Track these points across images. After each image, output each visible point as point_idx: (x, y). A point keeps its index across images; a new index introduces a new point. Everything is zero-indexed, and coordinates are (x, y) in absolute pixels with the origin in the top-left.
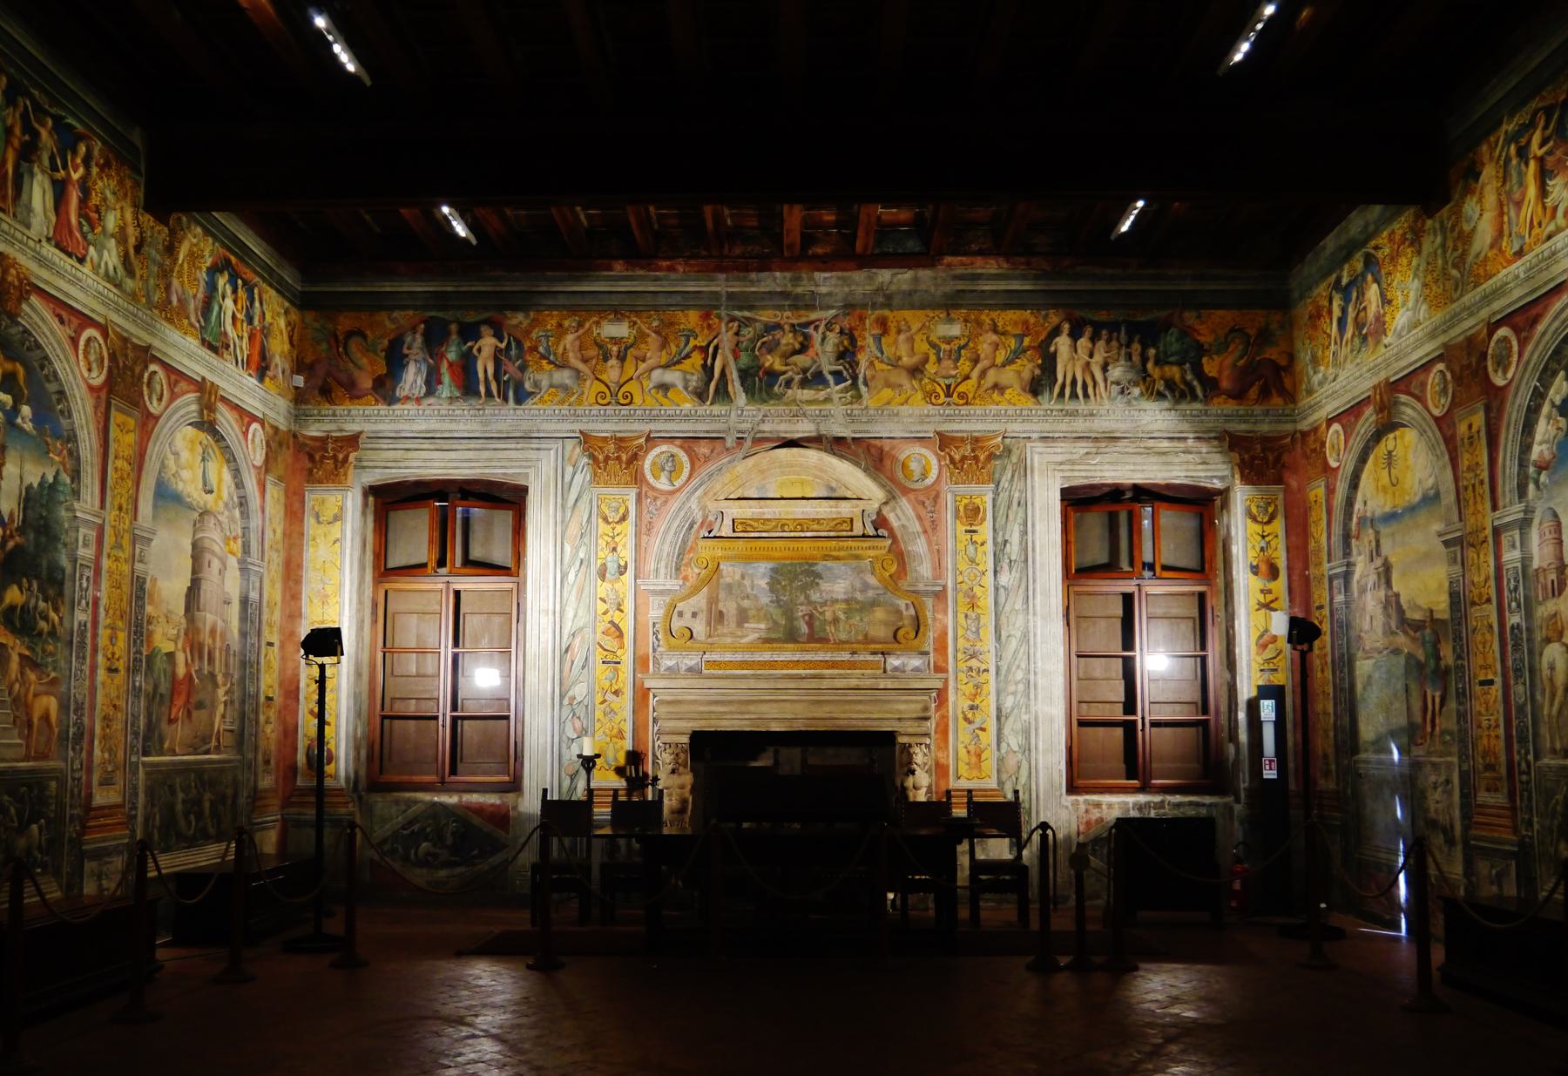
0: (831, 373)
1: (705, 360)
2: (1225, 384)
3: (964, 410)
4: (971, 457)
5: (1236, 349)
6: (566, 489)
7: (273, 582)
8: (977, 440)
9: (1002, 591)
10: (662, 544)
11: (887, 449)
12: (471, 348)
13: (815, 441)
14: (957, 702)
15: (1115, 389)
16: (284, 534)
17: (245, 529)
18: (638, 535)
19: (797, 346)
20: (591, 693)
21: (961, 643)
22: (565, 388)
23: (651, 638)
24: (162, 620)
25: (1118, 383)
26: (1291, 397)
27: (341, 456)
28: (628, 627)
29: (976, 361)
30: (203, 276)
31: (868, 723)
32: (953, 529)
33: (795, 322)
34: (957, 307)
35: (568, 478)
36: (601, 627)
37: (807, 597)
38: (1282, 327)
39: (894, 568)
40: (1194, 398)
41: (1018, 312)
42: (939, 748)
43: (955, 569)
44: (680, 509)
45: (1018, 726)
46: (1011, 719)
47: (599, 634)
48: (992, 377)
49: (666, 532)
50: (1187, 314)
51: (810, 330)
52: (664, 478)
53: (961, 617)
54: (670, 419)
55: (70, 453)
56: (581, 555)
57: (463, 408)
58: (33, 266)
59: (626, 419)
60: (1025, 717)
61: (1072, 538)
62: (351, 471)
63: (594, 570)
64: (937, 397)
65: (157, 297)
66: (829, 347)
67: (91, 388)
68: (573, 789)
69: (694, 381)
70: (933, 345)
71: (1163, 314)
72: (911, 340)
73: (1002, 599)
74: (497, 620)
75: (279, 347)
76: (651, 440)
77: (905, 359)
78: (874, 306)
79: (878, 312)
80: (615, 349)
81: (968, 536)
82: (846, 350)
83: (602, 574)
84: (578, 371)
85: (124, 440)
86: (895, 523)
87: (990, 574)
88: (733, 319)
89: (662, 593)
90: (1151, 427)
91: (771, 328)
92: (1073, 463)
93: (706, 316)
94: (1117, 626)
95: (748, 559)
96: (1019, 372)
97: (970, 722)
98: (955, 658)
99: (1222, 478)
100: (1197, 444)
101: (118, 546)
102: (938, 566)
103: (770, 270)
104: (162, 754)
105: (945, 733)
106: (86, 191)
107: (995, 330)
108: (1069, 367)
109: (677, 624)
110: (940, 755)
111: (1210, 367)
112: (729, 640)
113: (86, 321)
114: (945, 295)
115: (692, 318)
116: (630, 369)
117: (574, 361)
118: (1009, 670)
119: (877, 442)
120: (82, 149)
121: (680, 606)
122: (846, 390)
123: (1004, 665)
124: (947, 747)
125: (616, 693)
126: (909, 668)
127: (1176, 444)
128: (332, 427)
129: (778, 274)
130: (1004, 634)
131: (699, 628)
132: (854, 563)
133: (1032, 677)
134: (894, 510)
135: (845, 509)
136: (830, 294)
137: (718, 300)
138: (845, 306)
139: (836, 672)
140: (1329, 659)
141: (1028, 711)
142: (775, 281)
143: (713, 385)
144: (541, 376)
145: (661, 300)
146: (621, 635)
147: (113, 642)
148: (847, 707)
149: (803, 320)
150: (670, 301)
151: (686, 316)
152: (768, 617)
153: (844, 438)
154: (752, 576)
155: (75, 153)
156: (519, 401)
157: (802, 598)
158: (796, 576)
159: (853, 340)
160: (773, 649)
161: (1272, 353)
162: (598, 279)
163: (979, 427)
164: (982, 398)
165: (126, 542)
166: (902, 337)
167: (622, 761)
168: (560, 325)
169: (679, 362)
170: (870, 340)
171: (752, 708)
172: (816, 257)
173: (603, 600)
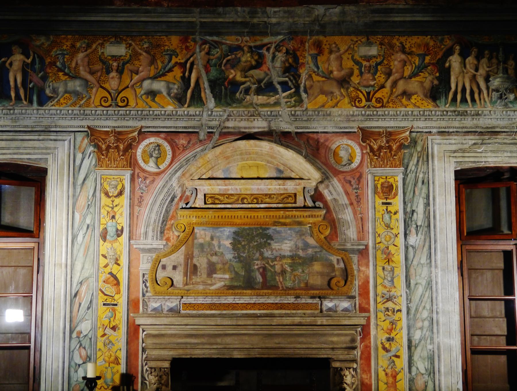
0: (280, 83)
4: (386, 147)
6: (76, 170)
8: (390, 134)
9: (410, 249)
10: (150, 213)
11: (322, 141)
12: (5, 62)
14: (377, 335)
15: (495, 95)
19: (254, 63)
20: (94, 329)
21: (380, 290)
22: (76, 93)
23: (141, 286)
25: (497, 90)
28: (123, 277)
29: (389, 74)
31: (308, 352)
32: (372, 202)
33: (252, 44)
34: (374, 33)
35: (78, 162)
37: (262, 254)
39: (328, 232)
41: (421, 38)
42: (364, 371)
43: (375, 233)
44: (164, 186)
45: (425, 354)
46: (419, 349)
47: (101, 283)
48: (401, 86)
51: (264, 51)
52: (152, 163)
53: (379, 269)
54: (156, 117)
56: (88, 221)
59: (124, 117)
60: (430, 347)
61: (464, 208)
63: (97, 233)
64: (360, 101)
66: (278, 64)
70: (357, 63)
72: (340, 58)
74: (22, 271)
76: (142, 134)
78: (312, 33)
80: (115, 64)
81: (384, 207)
82: (291, 66)
83: (104, 236)
84: (87, 81)
86: (329, 198)
87: (401, 236)
88: (205, 42)
89: (150, 251)
91: (233, 49)
92: (464, 151)
93: (184, 40)
95: (216, 225)
96: (422, 83)
97: (387, 350)
98: (376, 300)
102: (362, 231)
103: (233, 5)
105: (368, 359)
107: (403, 50)
108: (460, 78)
109: (161, 275)
110: (364, 376)
112: (201, 287)
115: (175, 41)
116: (126, 81)
117: (83, 73)
118: (417, 310)
119: (315, 136)
121: (164, 261)
122: (290, 96)
125: (114, 328)
126: (340, 309)
129: (239, 9)
130: (413, 282)
131: (178, 278)
132: (297, 228)
133: (435, 316)
134: (327, 187)
135: (290, 187)
136: (278, 24)
138: (290, 33)
139: (283, 312)
146: (118, 284)
148: (293, 339)
149: (258, 43)
151: (169, 40)
152: (231, 269)
153: (289, 133)
154: (219, 238)
156: (41, 103)
157: (257, 255)
158: (252, 238)
160: (235, 294)
163: (392, 124)
166: (333, 56)
168: (73, 46)
169: (164, 75)
170: (310, 59)
171: (219, 340)
173: (105, 256)
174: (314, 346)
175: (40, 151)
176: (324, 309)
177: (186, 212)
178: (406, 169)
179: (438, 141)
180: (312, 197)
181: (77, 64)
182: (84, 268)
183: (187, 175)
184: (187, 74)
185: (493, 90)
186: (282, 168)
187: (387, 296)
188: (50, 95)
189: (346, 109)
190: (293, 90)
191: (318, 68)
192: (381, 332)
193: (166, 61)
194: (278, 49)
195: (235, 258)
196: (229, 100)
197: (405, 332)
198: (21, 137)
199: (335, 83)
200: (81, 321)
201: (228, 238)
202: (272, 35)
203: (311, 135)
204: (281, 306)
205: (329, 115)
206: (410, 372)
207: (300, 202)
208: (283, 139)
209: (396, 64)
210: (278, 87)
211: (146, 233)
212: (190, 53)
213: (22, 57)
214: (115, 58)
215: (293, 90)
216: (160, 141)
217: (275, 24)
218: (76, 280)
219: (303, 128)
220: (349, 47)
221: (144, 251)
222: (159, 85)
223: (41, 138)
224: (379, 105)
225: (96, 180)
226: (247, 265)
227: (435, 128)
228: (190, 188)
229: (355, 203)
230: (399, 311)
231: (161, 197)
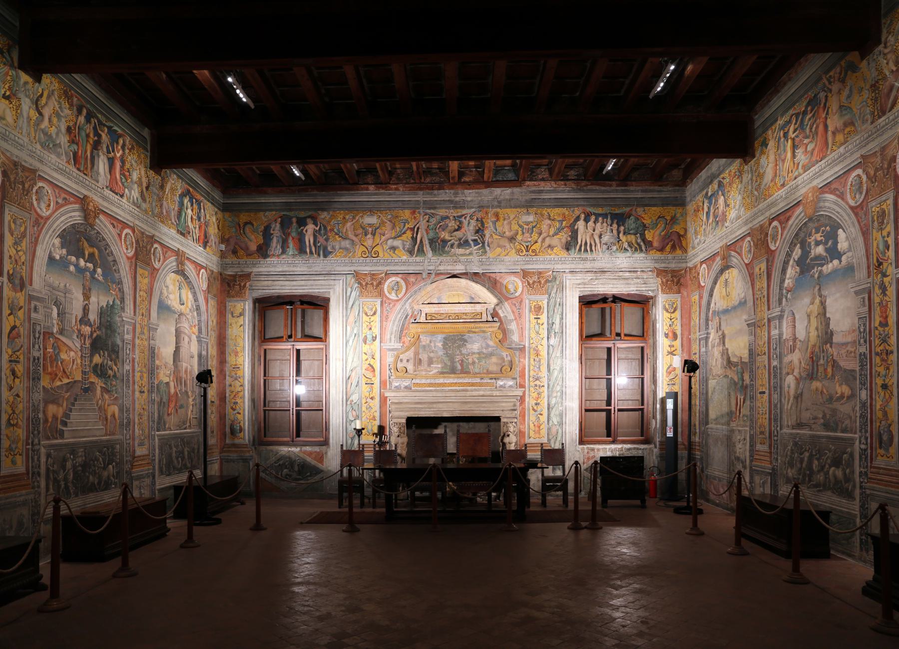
2: (655, 244)
3: (535, 258)
4: (539, 282)
5: (661, 226)
8: (540, 273)
10: (392, 326)
13: (464, 275)
14: (530, 401)
15: (605, 247)
17: (199, 321)
18: (381, 322)
20: (360, 399)
21: (532, 373)
22: (346, 249)
23: (388, 372)
24: (163, 367)
26: (685, 250)
28: (377, 367)
29: (540, 234)
30: (177, 199)
32: (528, 317)
34: (532, 207)
35: (348, 294)
36: (366, 366)
37: (461, 351)
39: (501, 337)
40: (641, 250)
43: (530, 337)
49: (394, 321)
50: (638, 209)
52: (393, 294)
53: (532, 360)
54: (396, 264)
55: (120, 290)
57: (299, 260)
58: (100, 201)
59: (376, 264)
61: (584, 321)
63: (361, 339)
65: (157, 211)
66: (471, 228)
67: (128, 258)
68: (352, 444)
69: (408, 245)
70: (520, 226)
71: (628, 209)
72: (510, 223)
73: (551, 352)
74: (316, 363)
75: (213, 231)
76: (388, 275)
78: (493, 207)
79: (495, 210)
83: (365, 341)
85: (143, 282)
87: (546, 339)
89: (392, 350)
90: (621, 266)
92: (585, 284)
94: (604, 362)
95: (433, 334)
97: (535, 411)
101: (143, 333)
102: (522, 335)
104: (165, 430)
105: (524, 416)
106: (123, 162)
109: (400, 365)
111: (649, 236)
113: (125, 225)
114: (526, 201)
116: (377, 241)
117: (351, 236)
119: (493, 275)
120: (121, 141)
121: (401, 356)
123: (551, 384)
125: (372, 398)
128: (238, 270)
130: (552, 368)
131: (410, 367)
132: (482, 334)
135: (478, 308)
136: (472, 201)
141: (562, 406)
144: (335, 243)
145: (392, 205)
146: (374, 371)
147: (140, 379)
150: (396, 205)
152: (442, 362)
155: (118, 143)
156: (325, 256)
158: (454, 341)
159: (483, 224)
160: (444, 377)
161: (677, 228)
162: (362, 195)
163: (542, 266)
165: (145, 331)
167: (376, 431)
169: (400, 236)
171: (435, 406)
172: (464, 182)
177: (415, 325)
182: (353, 361)
189: (513, 256)
194: (471, 217)
204: (473, 385)
207: (484, 319)
209: (544, 227)
214: (370, 225)
216: (398, 279)
221: (390, 350)
222: (397, 243)
226: (452, 359)
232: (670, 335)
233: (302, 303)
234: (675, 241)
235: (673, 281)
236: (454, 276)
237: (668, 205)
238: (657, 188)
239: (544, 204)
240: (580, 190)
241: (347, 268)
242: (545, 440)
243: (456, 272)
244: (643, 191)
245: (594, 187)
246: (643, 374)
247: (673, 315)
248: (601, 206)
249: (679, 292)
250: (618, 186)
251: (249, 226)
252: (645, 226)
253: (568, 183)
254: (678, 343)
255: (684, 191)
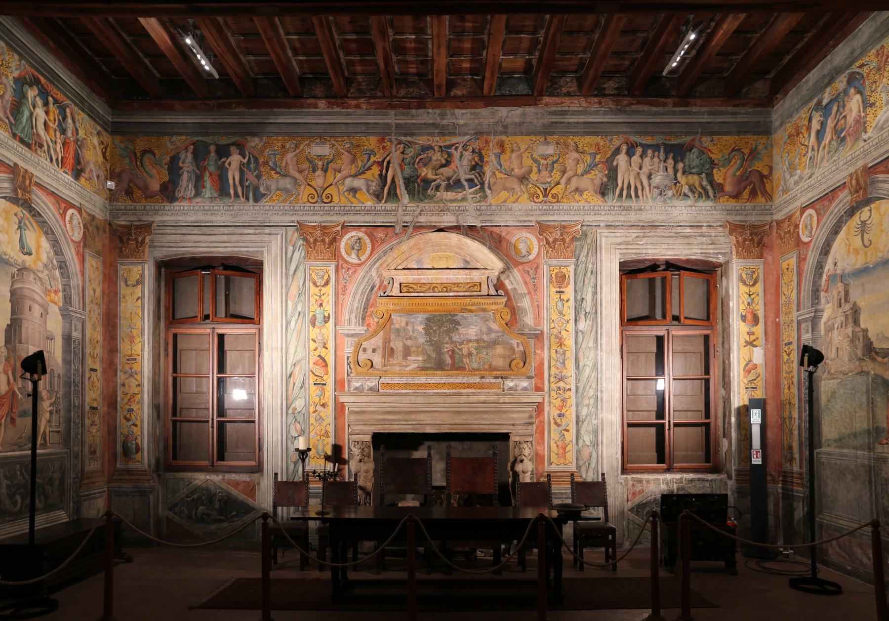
1: (381, 172)
2: (728, 188)
4: (562, 239)
5: (736, 163)
6: (289, 261)
7: (94, 328)
8: (564, 227)
9: (580, 334)
10: (352, 302)
11: (503, 234)
12: (224, 162)
13: (456, 229)
14: (551, 412)
15: (656, 191)
16: (103, 293)
19: (444, 162)
20: (307, 405)
21: (553, 371)
22: (287, 190)
23: (346, 367)
25: (658, 188)
26: (769, 197)
27: (140, 239)
31: (491, 427)
32: (548, 290)
33: (442, 144)
34: (552, 133)
35: (289, 255)
37: (450, 338)
38: (766, 148)
40: (708, 197)
41: (593, 138)
42: (538, 443)
43: (549, 319)
46: (586, 423)
47: (311, 365)
48: (574, 182)
49: (355, 294)
50: (704, 139)
51: (453, 150)
52: (354, 256)
53: (553, 352)
54: (357, 212)
56: (299, 309)
57: (219, 205)
59: (329, 213)
60: (595, 422)
62: (147, 249)
63: (307, 319)
64: (538, 197)
66: (465, 162)
68: (295, 472)
69: (374, 186)
70: (536, 161)
71: (688, 139)
72: (520, 157)
76: (345, 228)
77: (516, 170)
80: (320, 163)
82: (477, 164)
83: (313, 323)
84: (296, 179)
86: (509, 287)
87: (572, 322)
89: (353, 336)
93: (382, 140)
95: (410, 312)
97: (558, 425)
98: (549, 381)
99: (724, 254)
100: (709, 230)
102: (538, 316)
103: (425, 108)
105: (542, 433)
107: (577, 151)
108: (626, 176)
109: (362, 357)
111: (718, 177)
114: (544, 125)
117: (293, 172)
118: (584, 389)
121: (365, 344)
122: (476, 192)
124: (543, 443)
125: (323, 405)
126: (520, 388)
127: (695, 230)
128: (134, 218)
129: (430, 111)
131: (377, 360)
132: (482, 314)
133: (599, 394)
134: (508, 277)
135: (476, 276)
136: (465, 125)
137: (389, 129)
138: (476, 134)
139: (470, 391)
140: (795, 380)
141: (597, 418)
142: (426, 116)
143: (386, 188)
144: (270, 182)
145: (351, 129)
146: (326, 365)
148: (478, 416)
149: (448, 143)
150: (357, 130)
151: (368, 140)
152: (425, 352)
154: (413, 323)
156: (256, 200)
157: (447, 339)
158: (442, 323)
159: (481, 157)
160: (427, 375)
161: (758, 166)
162: (309, 114)
163: (566, 218)
164: (568, 198)
166: (514, 155)
167: (329, 453)
169: (363, 173)
170: (493, 157)
171: (413, 417)
172: (456, 97)
174: (497, 422)
175: (256, 244)
176: (506, 388)
177: (384, 300)
178: (578, 260)
179: (605, 234)
180: (495, 286)
181: (287, 163)
182: (296, 352)
183: (385, 265)
184: (384, 172)
185: (654, 187)
186: (468, 259)
187: (559, 377)
188: (264, 192)
189: (525, 203)
190: (478, 187)
191: (501, 166)
192: (553, 409)
193: (366, 160)
194: (465, 148)
195: (427, 341)
196: (421, 196)
197: (573, 408)
198: (239, 232)
199: (516, 180)
200: (295, 399)
201: (421, 323)
202: (460, 135)
203: (494, 229)
204: (468, 386)
205: (511, 210)
206: (577, 444)
207: (484, 291)
208: (469, 233)
209: (570, 163)
210: (465, 183)
211: (350, 320)
212: (387, 153)
213: (239, 157)
214: (320, 157)
215: (478, 187)
216: (361, 234)
217: (463, 125)
218: (290, 363)
219: (486, 222)
220: (529, 146)
221: (348, 335)
222: (359, 183)
223: (257, 232)
224: (554, 200)
225: (305, 270)
226: (438, 349)
227: (602, 222)
228: (387, 277)
229: (532, 292)
230: (570, 389)
231: (363, 286)
232: (749, 317)
233: (226, 267)
234: (756, 184)
235: (752, 240)
236: (441, 230)
237: (746, 133)
238: (731, 109)
239: (570, 130)
240: (620, 112)
241: (288, 218)
242: (573, 468)
243: (443, 225)
244: (711, 113)
245: (641, 107)
246: (707, 372)
247: (753, 290)
248: (652, 134)
249: (761, 256)
250: (675, 105)
251: (149, 155)
252: (712, 162)
253: (603, 100)
254: (759, 329)
255: (769, 113)
